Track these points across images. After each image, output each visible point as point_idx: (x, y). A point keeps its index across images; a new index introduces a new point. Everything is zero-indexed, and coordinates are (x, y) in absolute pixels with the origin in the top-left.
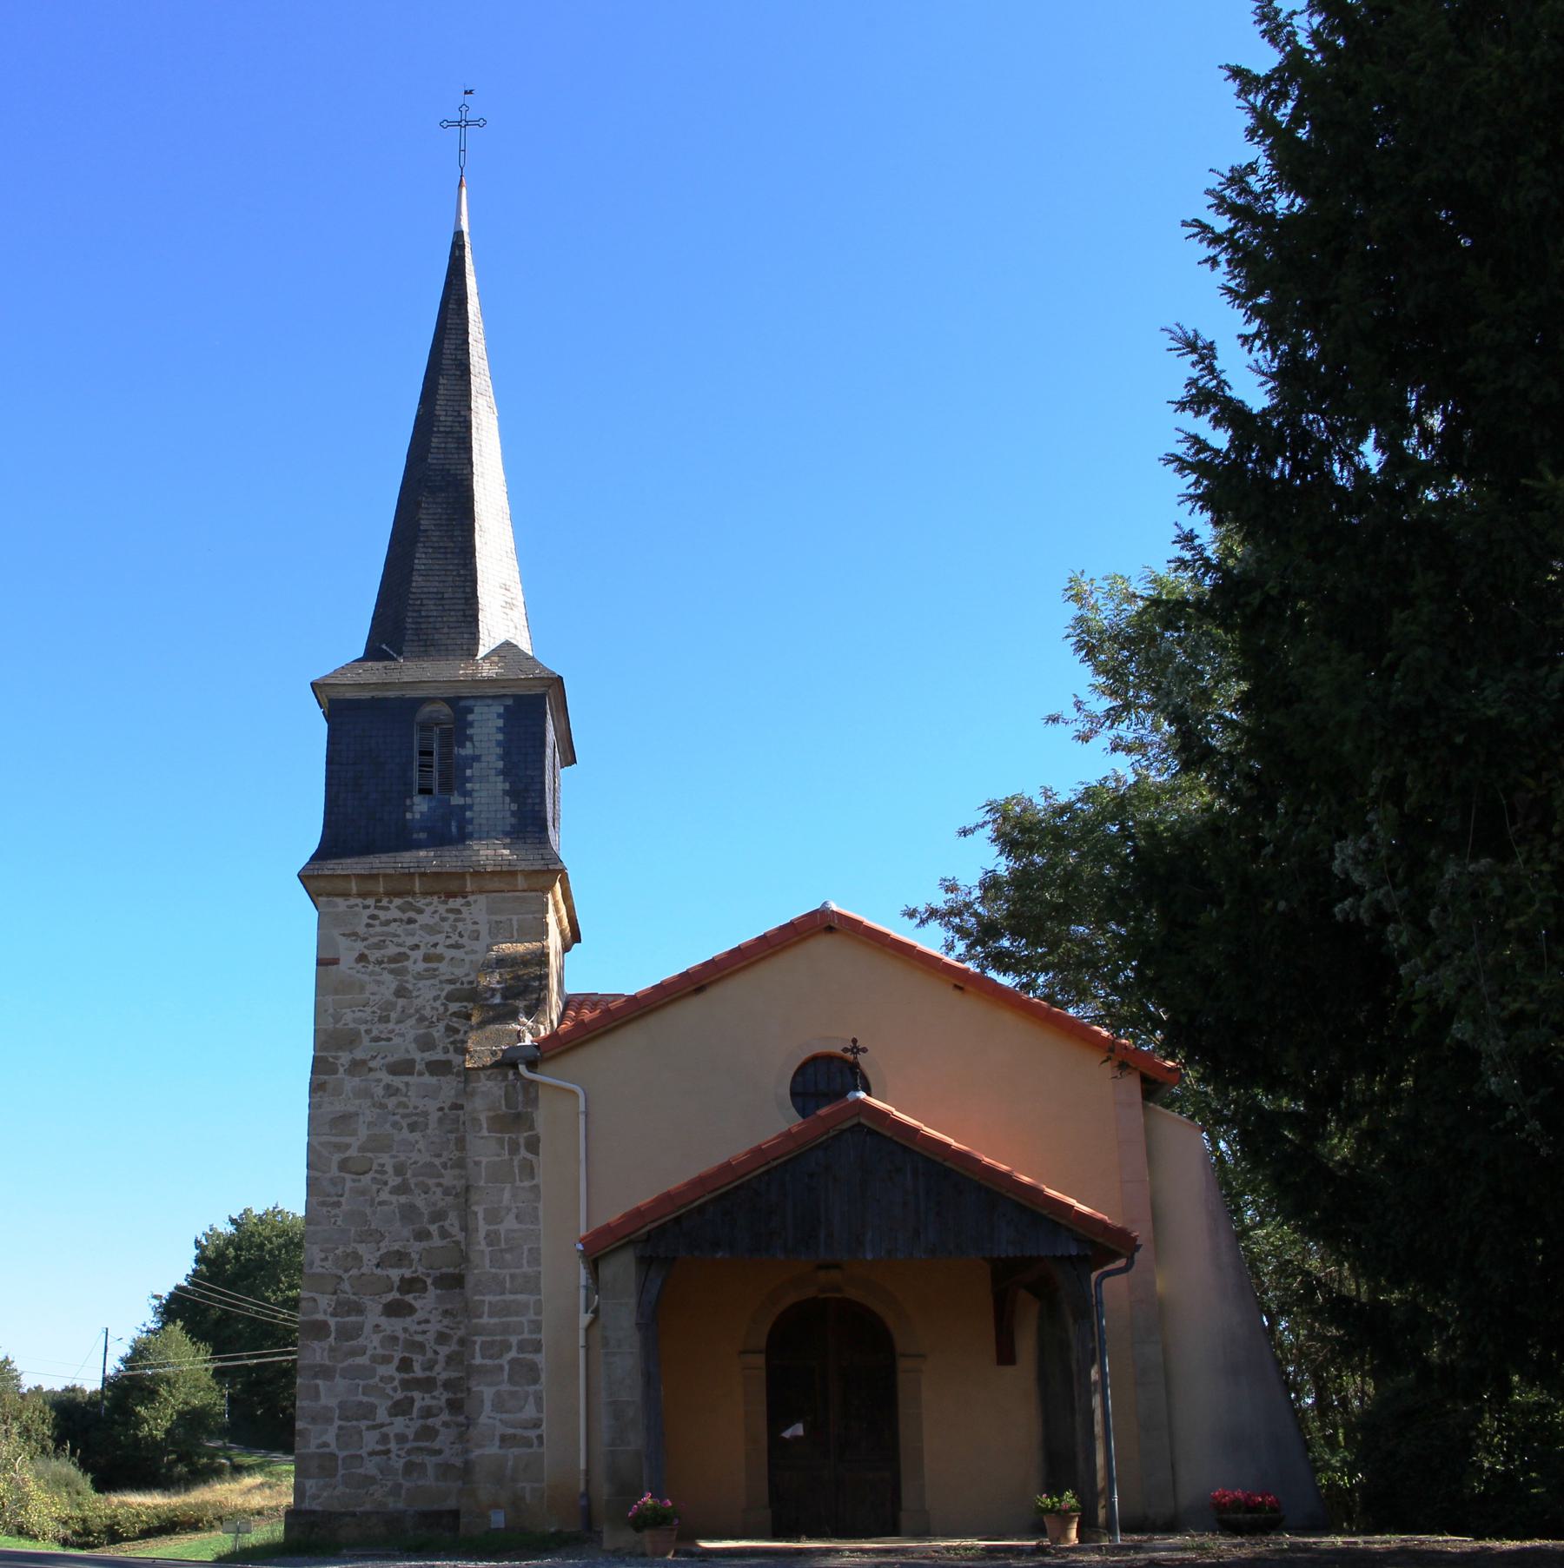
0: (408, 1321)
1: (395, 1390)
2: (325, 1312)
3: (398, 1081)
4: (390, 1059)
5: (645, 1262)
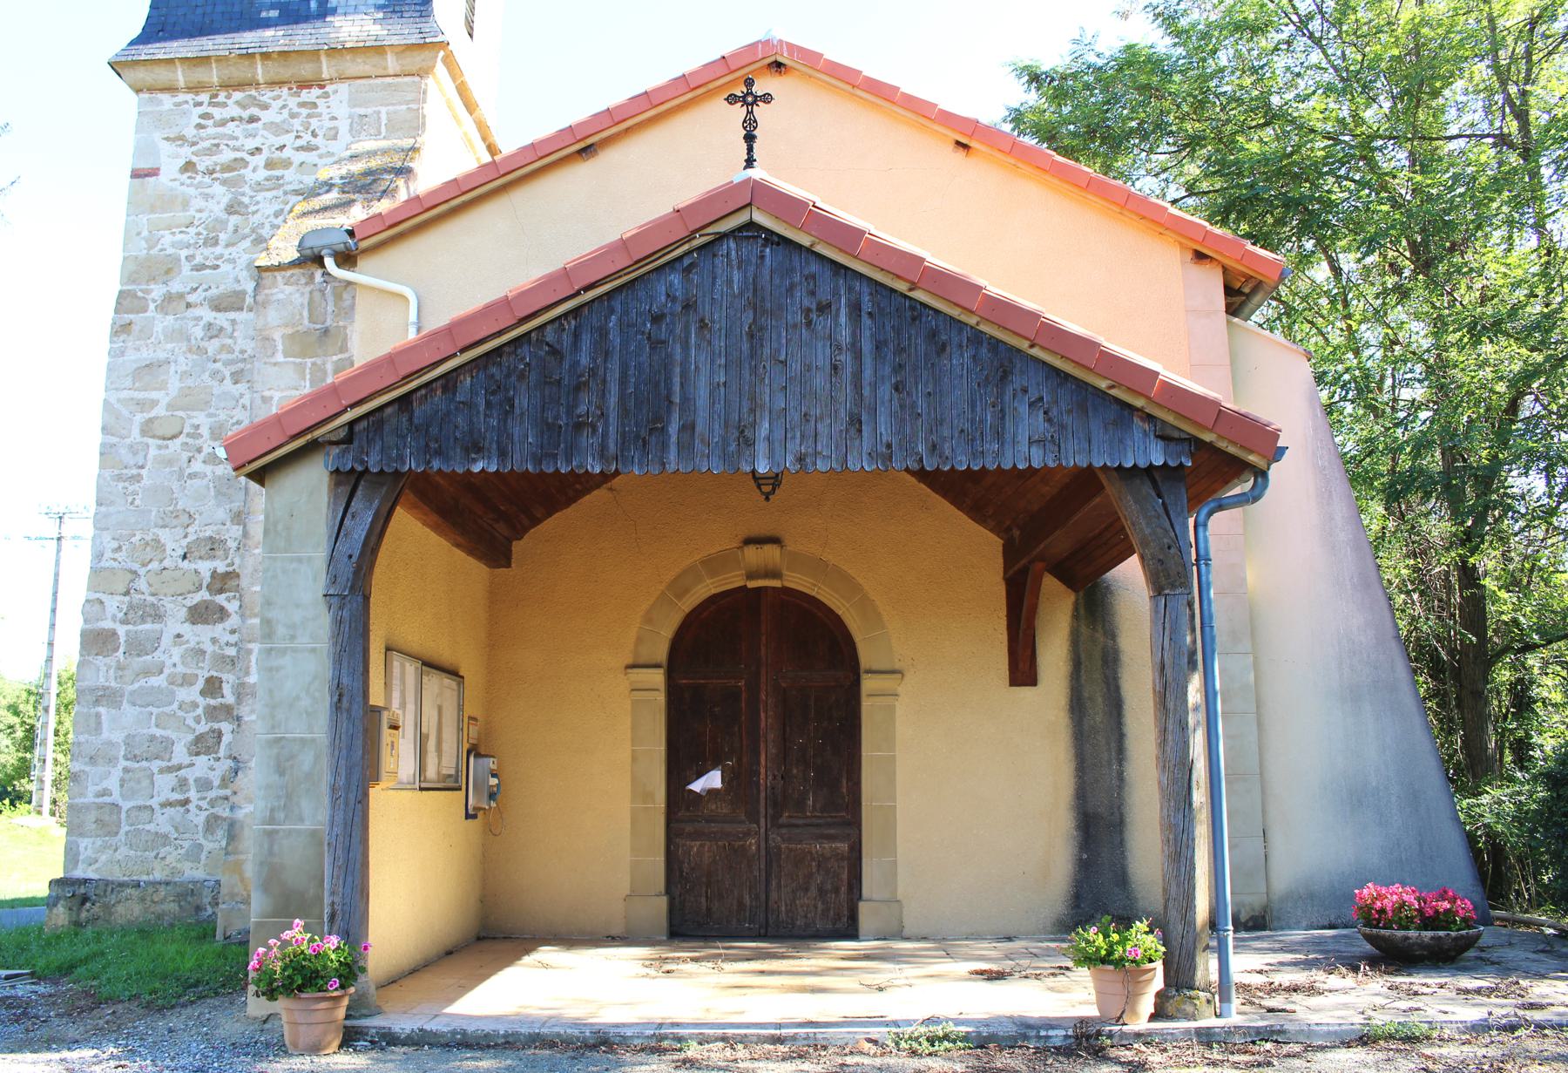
0: (219, 630)
1: (198, 720)
2: (114, 618)
3: (222, 319)
4: (214, 292)
5: (348, 481)
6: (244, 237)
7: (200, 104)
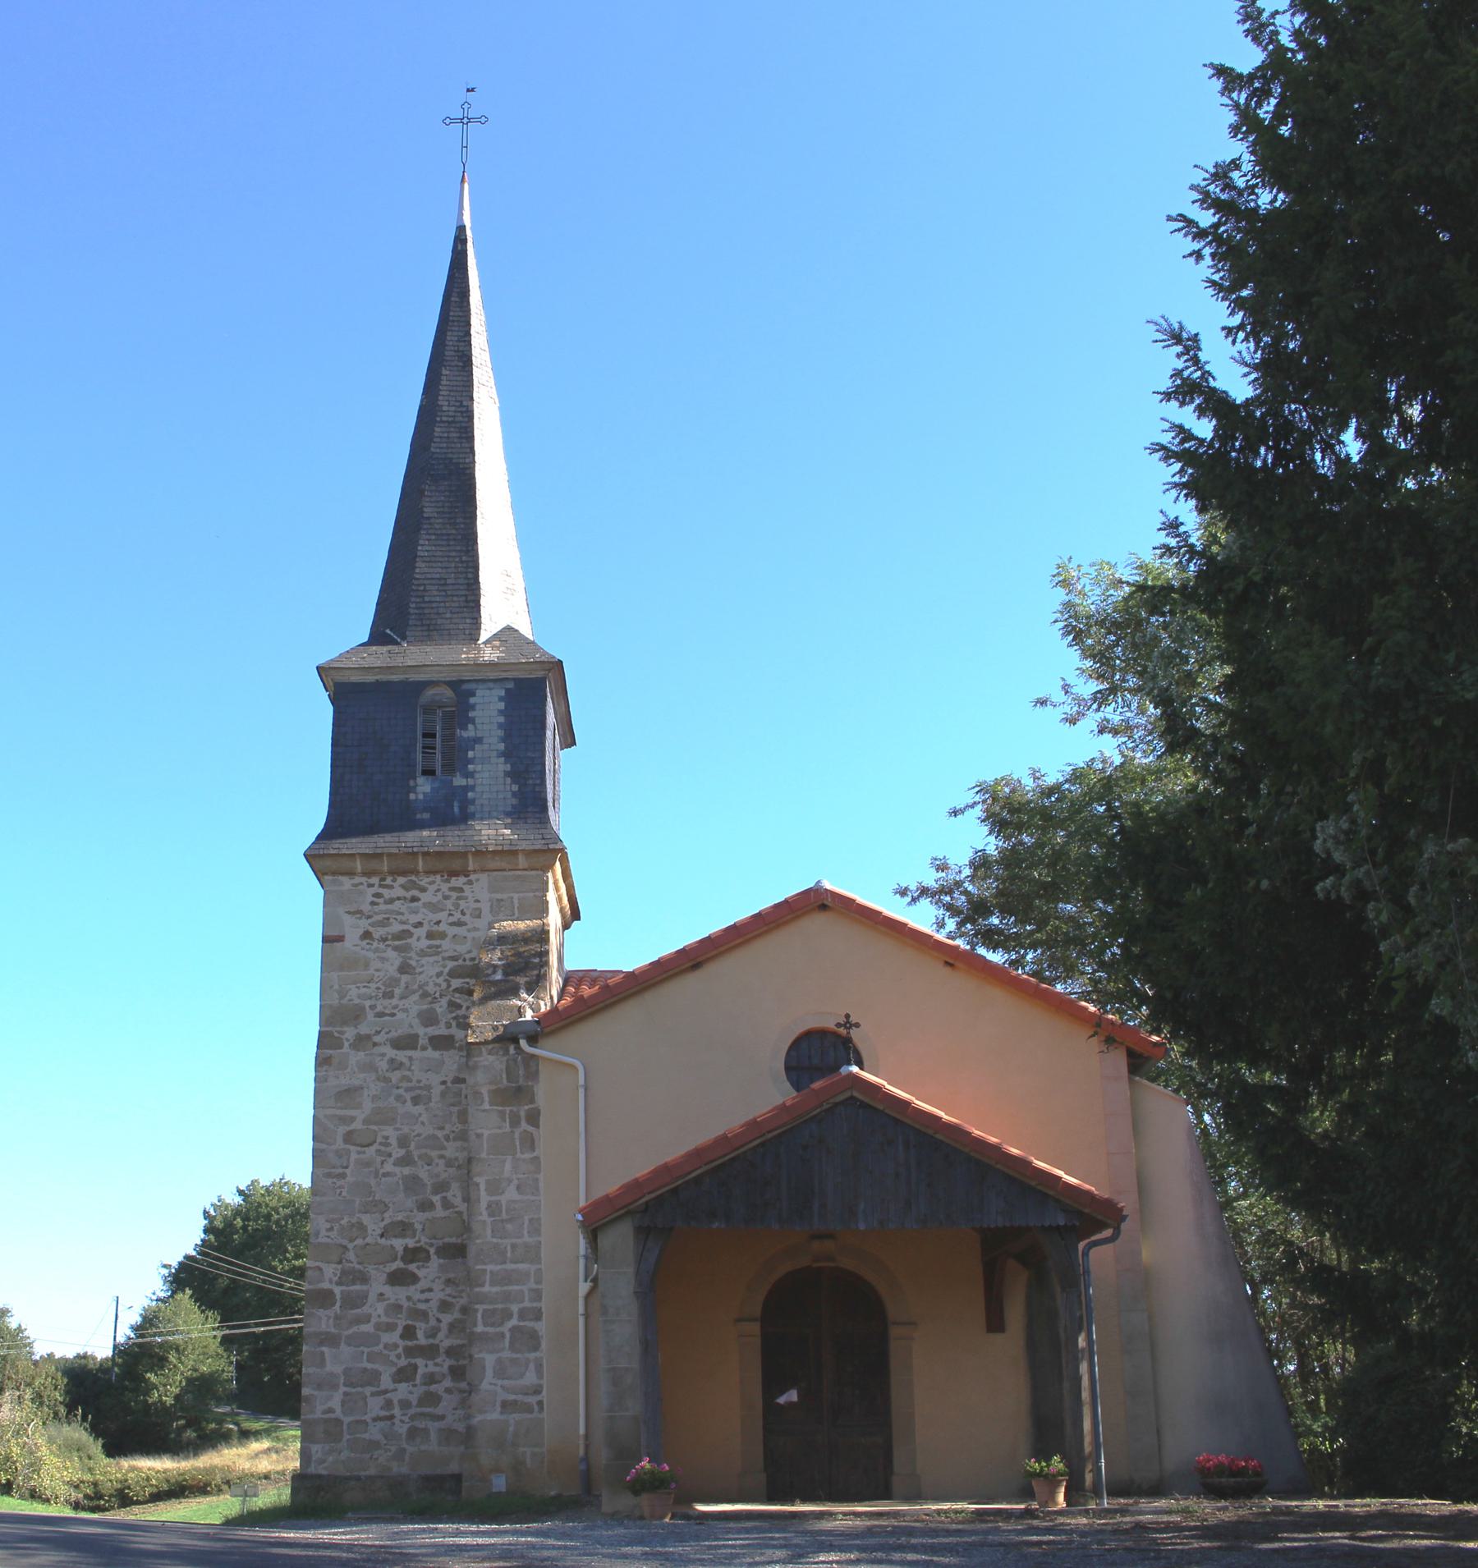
0: (412, 1291)
1: (398, 1357)
2: (331, 1281)
3: (401, 1056)
4: (394, 1034)
5: (643, 1233)
6: (414, 992)
7: (372, 885)
